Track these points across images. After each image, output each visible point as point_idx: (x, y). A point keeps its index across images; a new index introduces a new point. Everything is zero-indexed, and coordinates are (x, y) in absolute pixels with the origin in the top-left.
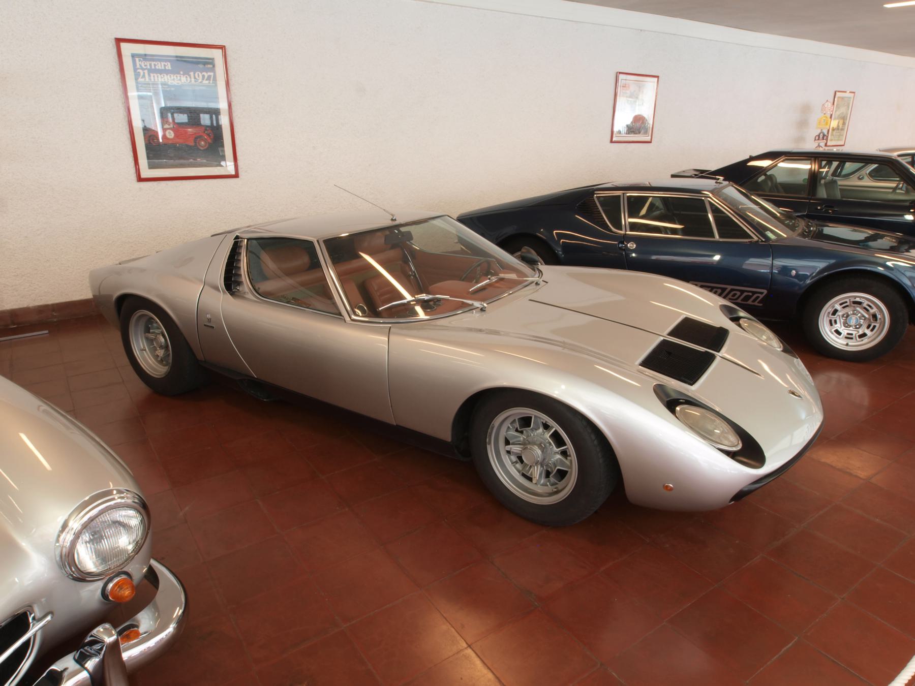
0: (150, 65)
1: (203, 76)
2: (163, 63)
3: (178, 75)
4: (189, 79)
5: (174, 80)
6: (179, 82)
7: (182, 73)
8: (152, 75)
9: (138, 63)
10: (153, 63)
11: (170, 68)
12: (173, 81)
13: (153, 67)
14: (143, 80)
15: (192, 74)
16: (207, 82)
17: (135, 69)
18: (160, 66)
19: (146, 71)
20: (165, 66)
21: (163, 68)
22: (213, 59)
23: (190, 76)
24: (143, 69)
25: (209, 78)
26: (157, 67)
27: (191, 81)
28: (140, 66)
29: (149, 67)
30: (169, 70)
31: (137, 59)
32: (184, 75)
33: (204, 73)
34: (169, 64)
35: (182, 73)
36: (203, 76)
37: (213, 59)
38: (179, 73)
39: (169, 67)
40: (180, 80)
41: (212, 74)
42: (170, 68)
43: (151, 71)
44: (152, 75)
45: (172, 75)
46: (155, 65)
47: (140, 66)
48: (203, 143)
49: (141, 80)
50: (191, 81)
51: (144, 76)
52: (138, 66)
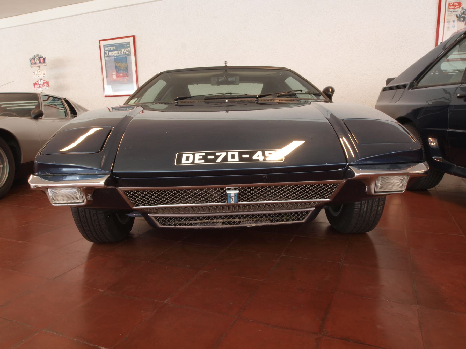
1: (126, 50)
2: (113, 47)
3: (118, 51)
4: (121, 51)
5: (116, 53)
6: (118, 54)
8: (109, 53)
9: (105, 48)
10: (110, 48)
11: (115, 49)
12: (116, 54)
13: (110, 49)
14: (107, 55)
15: (122, 50)
16: (128, 53)
17: (104, 51)
18: (112, 48)
19: (108, 51)
20: (113, 48)
21: (113, 49)
22: (129, 42)
23: (121, 51)
24: (107, 51)
25: (128, 50)
26: (111, 49)
27: (122, 53)
28: (106, 50)
29: (108, 50)
30: (115, 50)
31: (105, 47)
32: (119, 51)
33: (127, 49)
34: (115, 47)
35: (119, 50)
36: (126, 50)
37: (129, 42)
38: (118, 50)
39: (115, 49)
40: (118, 53)
41: (129, 49)
42: (115, 49)
43: (110, 51)
44: (109, 53)
45: (116, 52)
46: (110, 48)
47: (106, 50)
48: (126, 80)
49: (106, 55)
50: (122, 53)
51: (107, 54)
52: (105, 50)
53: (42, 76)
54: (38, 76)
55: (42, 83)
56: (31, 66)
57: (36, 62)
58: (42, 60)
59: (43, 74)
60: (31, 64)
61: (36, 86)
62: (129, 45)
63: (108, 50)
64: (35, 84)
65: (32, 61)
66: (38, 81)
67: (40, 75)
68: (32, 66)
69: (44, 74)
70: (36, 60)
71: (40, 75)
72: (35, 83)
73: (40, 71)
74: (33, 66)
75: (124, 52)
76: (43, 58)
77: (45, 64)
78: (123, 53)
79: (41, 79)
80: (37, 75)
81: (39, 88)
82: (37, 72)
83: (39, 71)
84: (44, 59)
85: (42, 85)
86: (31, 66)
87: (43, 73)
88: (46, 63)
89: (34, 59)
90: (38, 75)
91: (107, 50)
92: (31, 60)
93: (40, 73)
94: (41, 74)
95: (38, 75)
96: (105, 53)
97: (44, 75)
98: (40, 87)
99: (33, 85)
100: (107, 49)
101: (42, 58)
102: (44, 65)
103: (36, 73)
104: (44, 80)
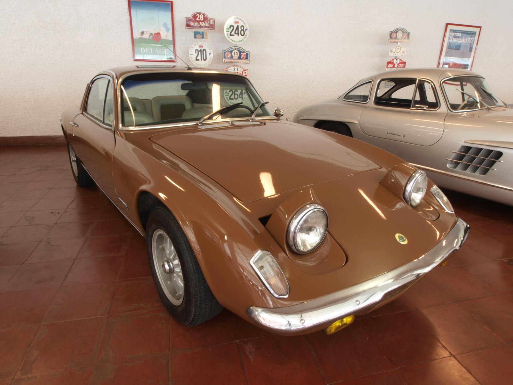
0: (455, 34)
7: (464, 38)
8: (454, 38)
10: (456, 33)
13: (455, 35)
15: (467, 38)
17: (450, 36)
19: (452, 37)
22: (476, 32)
23: (466, 39)
25: (472, 39)
29: (454, 35)
35: (464, 38)
36: (471, 39)
37: (476, 32)
41: (473, 39)
46: (456, 34)
47: (451, 35)
53: (399, 55)
54: (396, 54)
55: (398, 62)
56: (390, 40)
57: (398, 36)
58: (405, 36)
59: (402, 53)
60: (391, 38)
61: (390, 66)
62: (474, 35)
63: (453, 36)
64: (389, 63)
65: (392, 34)
66: (393, 60)
67: (398, 53)
68: (390, 41)
69: (403, 53)
70: (398, 34)
71: (398, 53)
72: (389, 61)
73: (399, 48)
74: (392, 40)
75: (467, 41)
76: (407, 34)
77: (408, 41)
78: (466, 42)
79: (396, 58)
80: (394, 52)
81: (392, 68)
82: (396, 49)
83: (398, 48)
84: (409, 34)
85: (397, 65)
86: (390, 40)
87: (402, 51)
88: (409, 40)
89: (396, 33)
90: (396, 53)
91: (452, 35)
92: (391, 33)
93: (399, 51)
94: (400, 52)
95: (396, 53)
96: (449, 38)
97: (403, 54)
98: (394, 67)
99: (386, 63)
100: (453, 34)
101: (406, 33)
102: (407, 43)
103: (394, 50)
104: (401, 60)
